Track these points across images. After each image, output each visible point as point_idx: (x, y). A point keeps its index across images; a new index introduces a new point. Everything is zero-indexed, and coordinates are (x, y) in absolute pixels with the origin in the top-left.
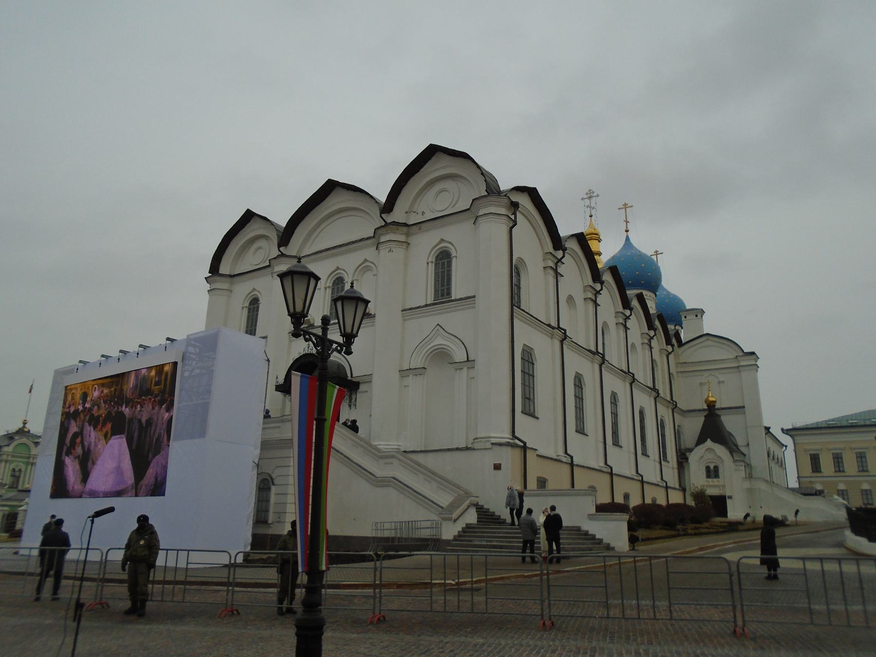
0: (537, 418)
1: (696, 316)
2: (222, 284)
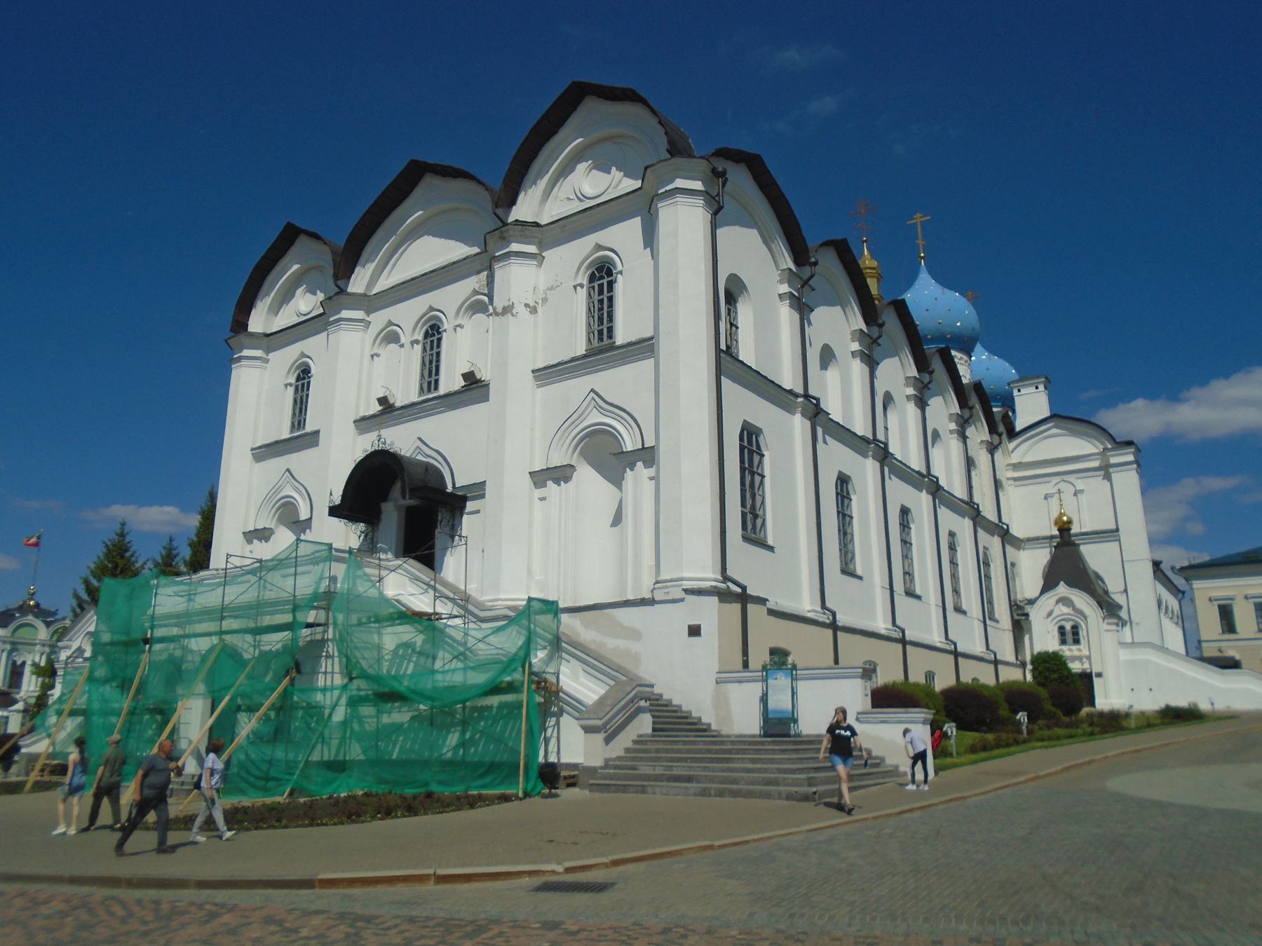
0: (771, 549)
1: (1037, 388)
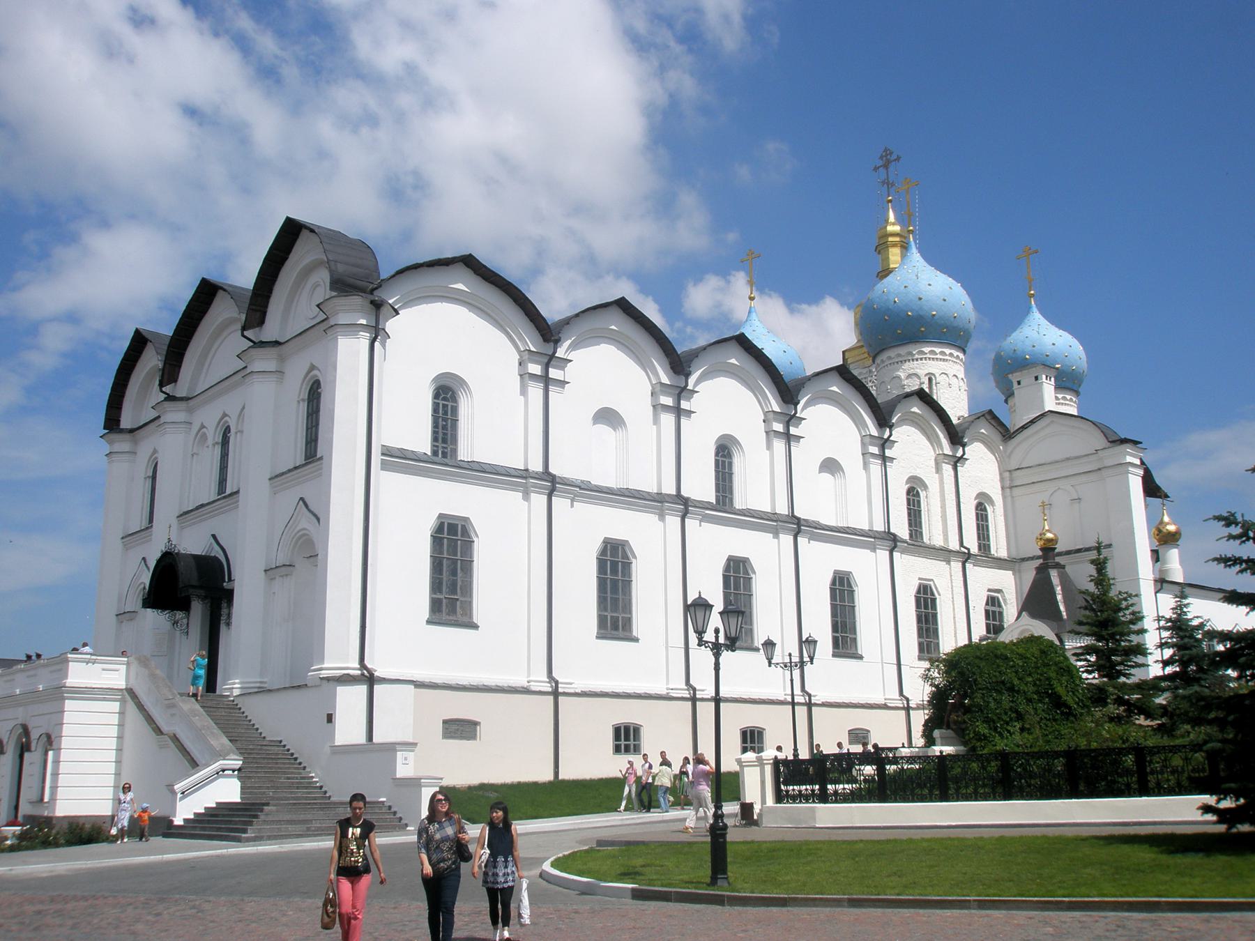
1: (1036, 378)
2: (122, 444)
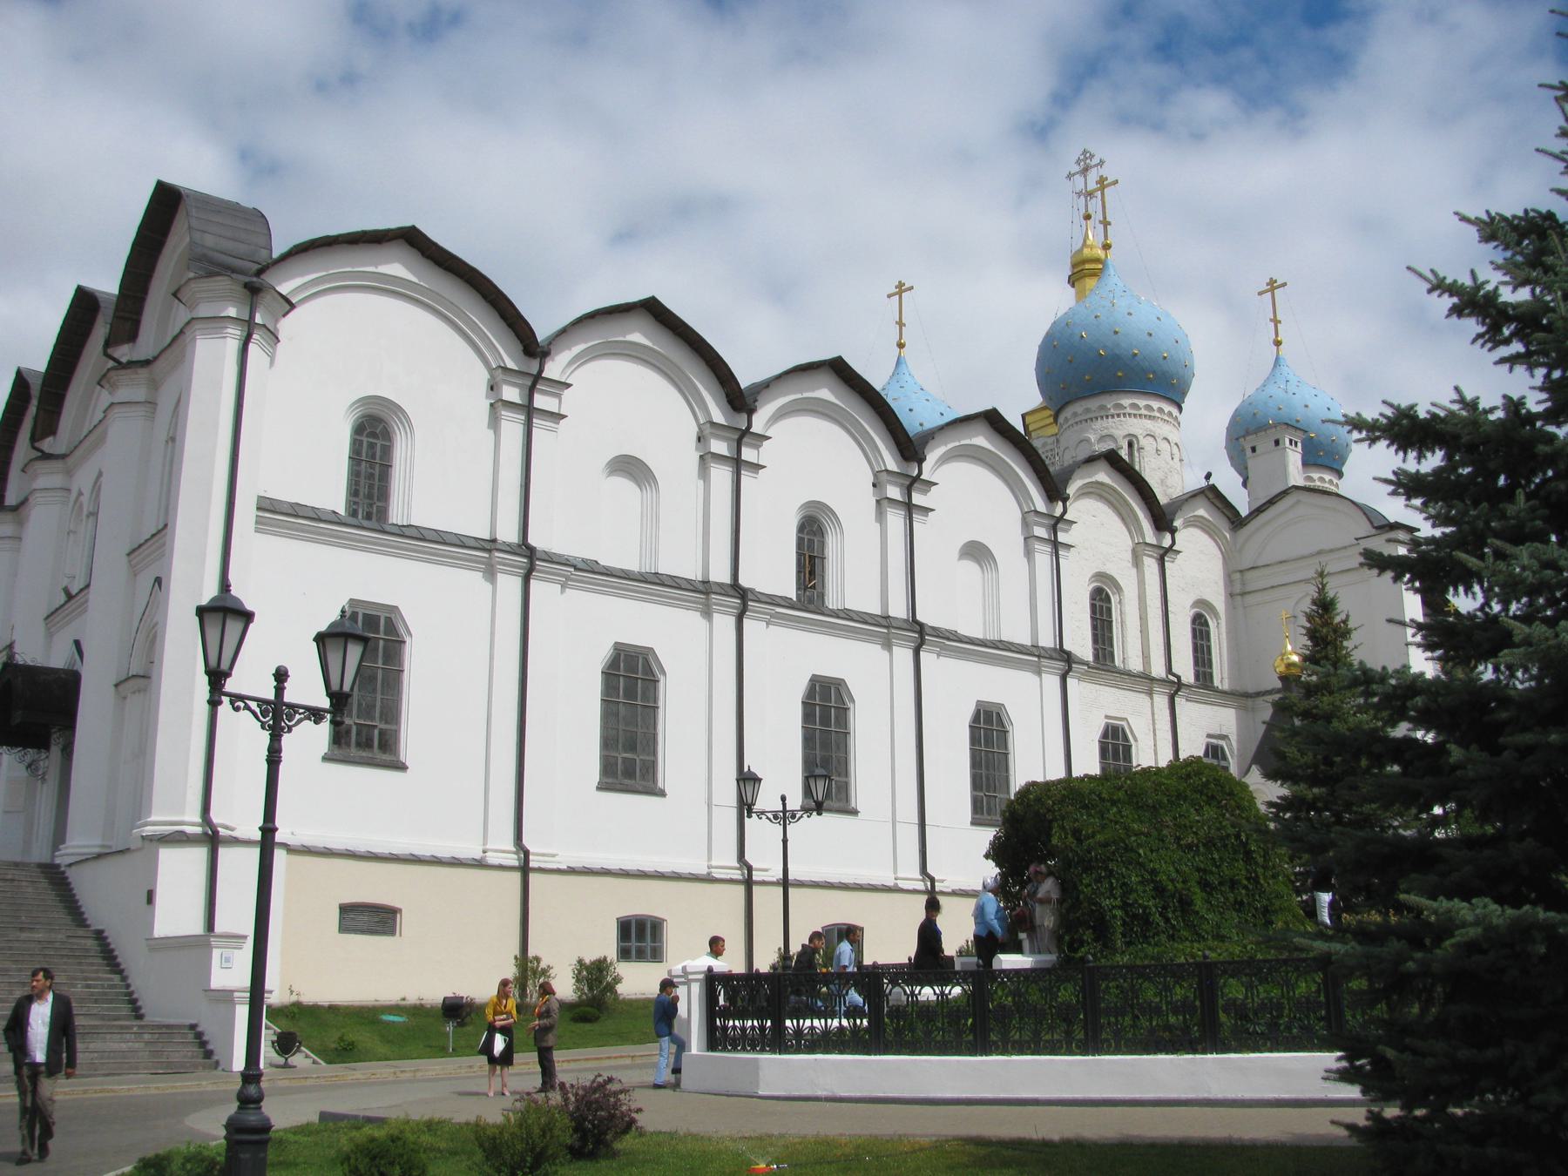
1: (1277, 443)
